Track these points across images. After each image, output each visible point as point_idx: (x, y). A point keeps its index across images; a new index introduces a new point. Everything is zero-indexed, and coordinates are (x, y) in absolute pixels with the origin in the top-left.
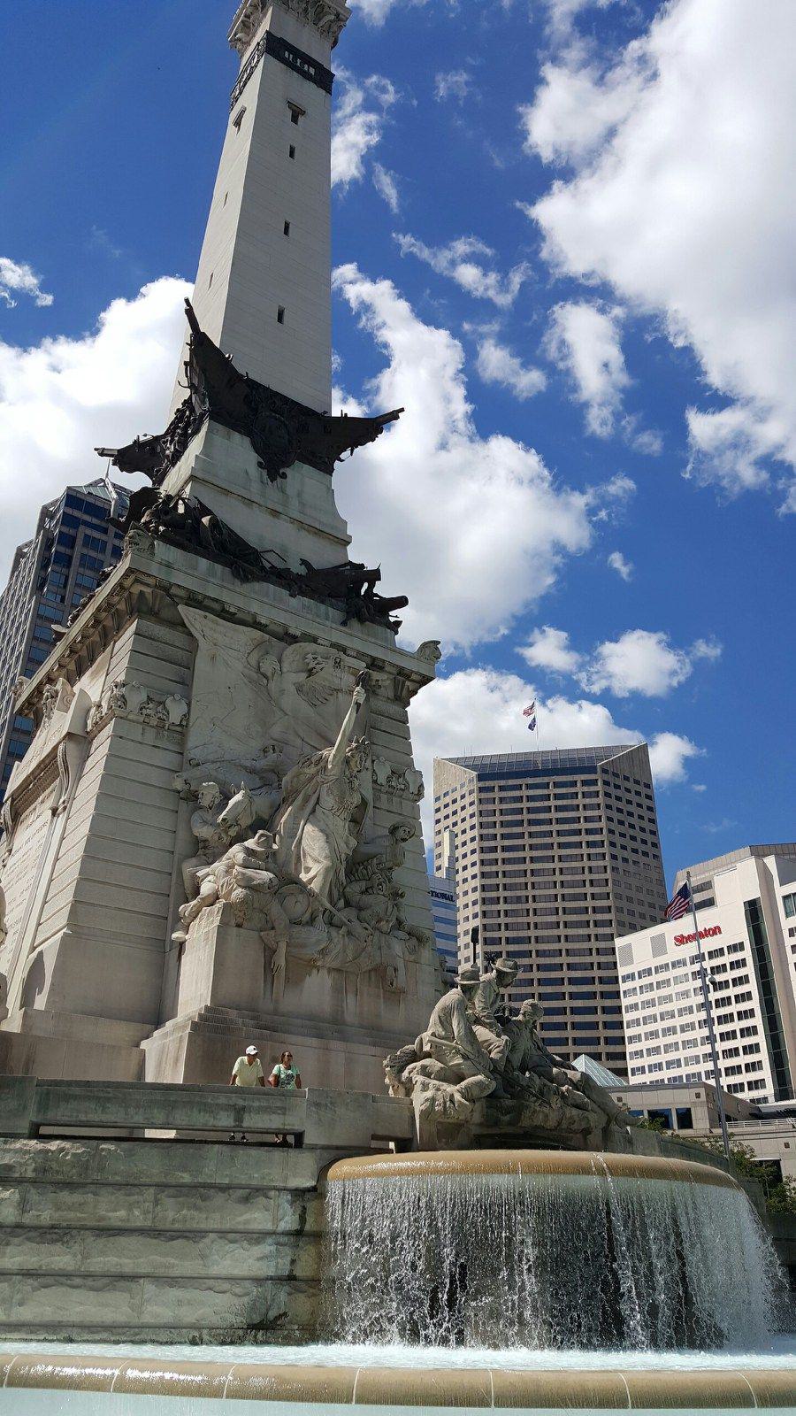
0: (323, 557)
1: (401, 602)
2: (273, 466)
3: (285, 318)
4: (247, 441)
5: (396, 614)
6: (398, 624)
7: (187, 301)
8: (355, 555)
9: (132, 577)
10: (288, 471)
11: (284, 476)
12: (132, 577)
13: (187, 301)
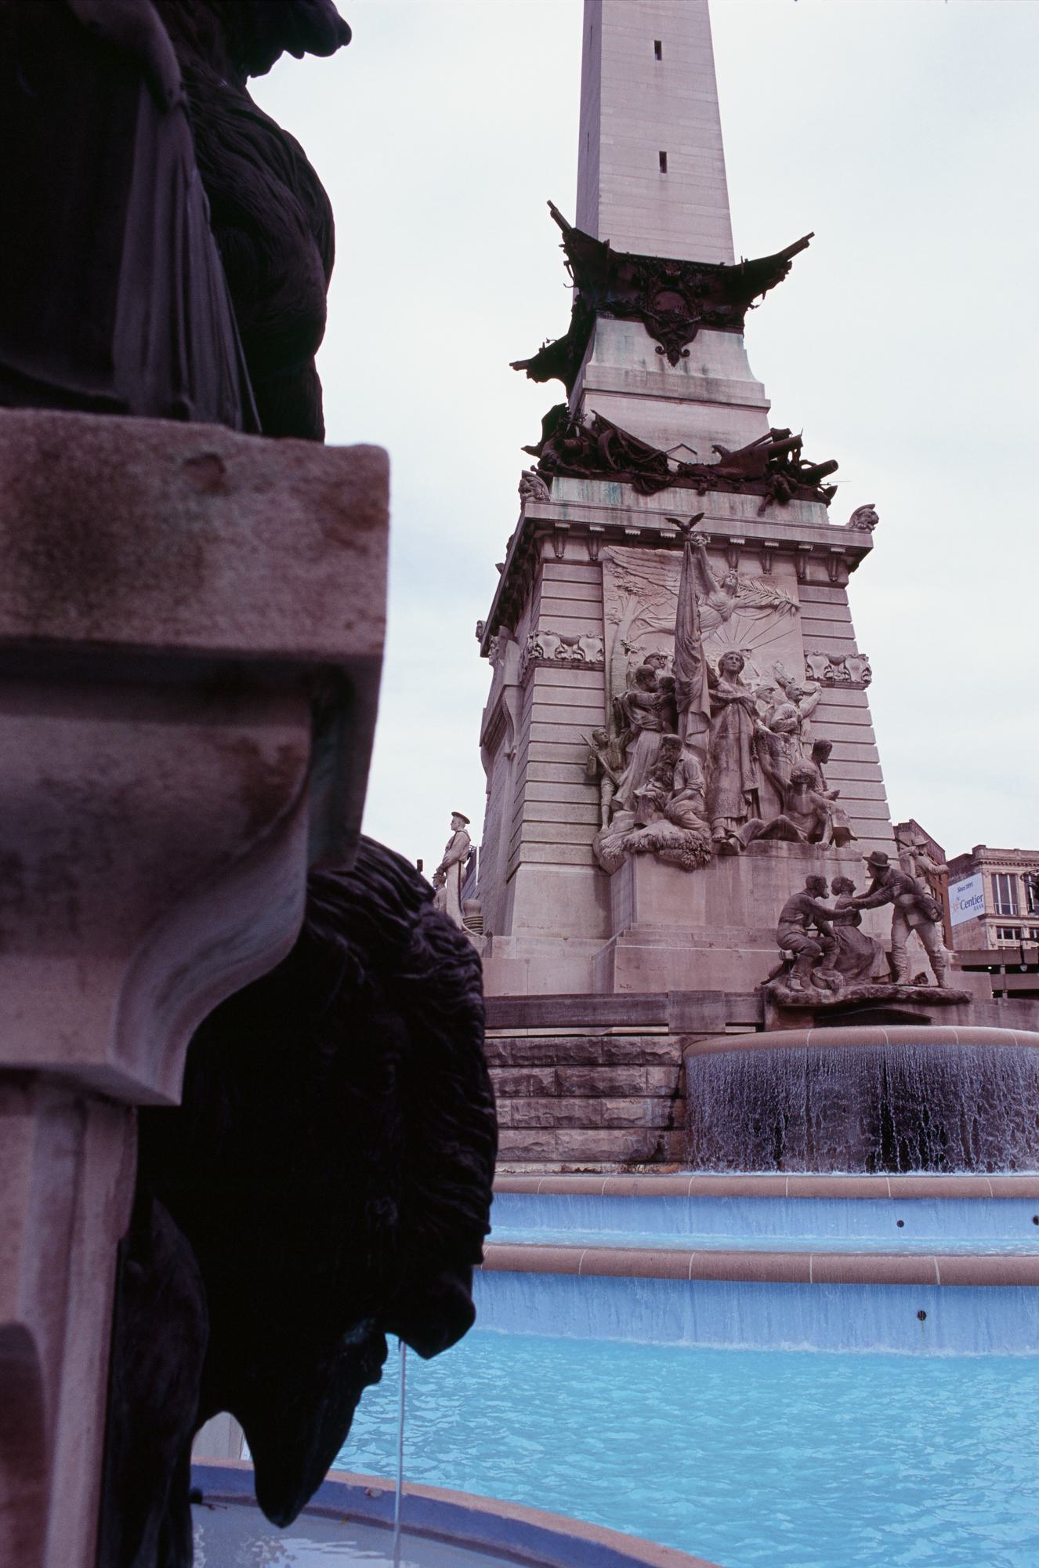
0: (742, 434)
1: (831, 467)
2: (673, 342)
3: (669, 164)
4: (642, 325)
5: (826, 481)
6: (832, 491)
7: (550, 203)
8: (776, 420)
9: (532, 527)
10: (691, 347)
11: (687, 353)
12: (532, 527)
13: (550, 203)
